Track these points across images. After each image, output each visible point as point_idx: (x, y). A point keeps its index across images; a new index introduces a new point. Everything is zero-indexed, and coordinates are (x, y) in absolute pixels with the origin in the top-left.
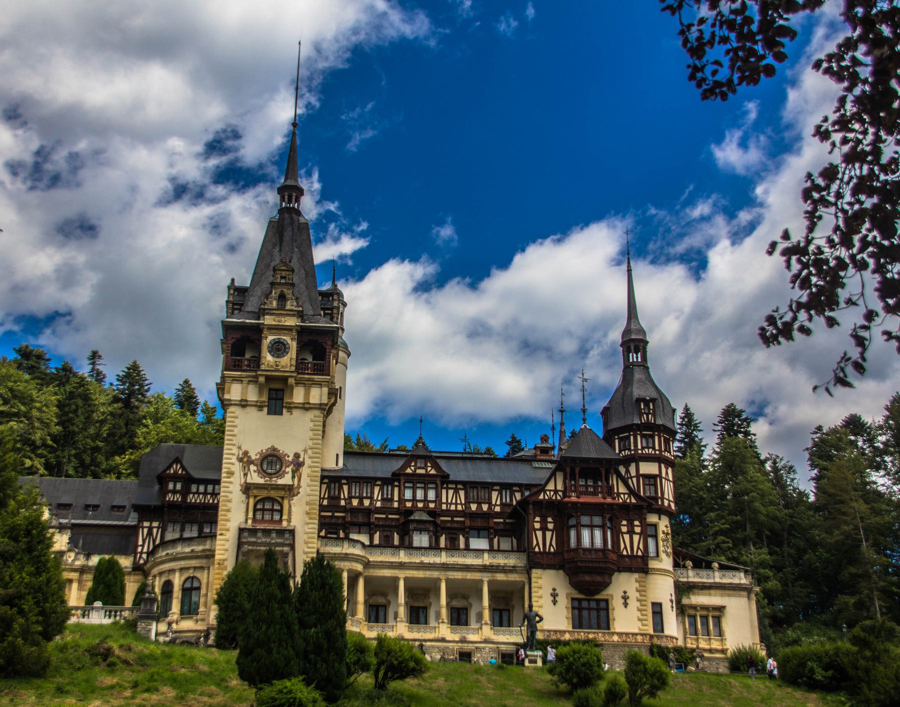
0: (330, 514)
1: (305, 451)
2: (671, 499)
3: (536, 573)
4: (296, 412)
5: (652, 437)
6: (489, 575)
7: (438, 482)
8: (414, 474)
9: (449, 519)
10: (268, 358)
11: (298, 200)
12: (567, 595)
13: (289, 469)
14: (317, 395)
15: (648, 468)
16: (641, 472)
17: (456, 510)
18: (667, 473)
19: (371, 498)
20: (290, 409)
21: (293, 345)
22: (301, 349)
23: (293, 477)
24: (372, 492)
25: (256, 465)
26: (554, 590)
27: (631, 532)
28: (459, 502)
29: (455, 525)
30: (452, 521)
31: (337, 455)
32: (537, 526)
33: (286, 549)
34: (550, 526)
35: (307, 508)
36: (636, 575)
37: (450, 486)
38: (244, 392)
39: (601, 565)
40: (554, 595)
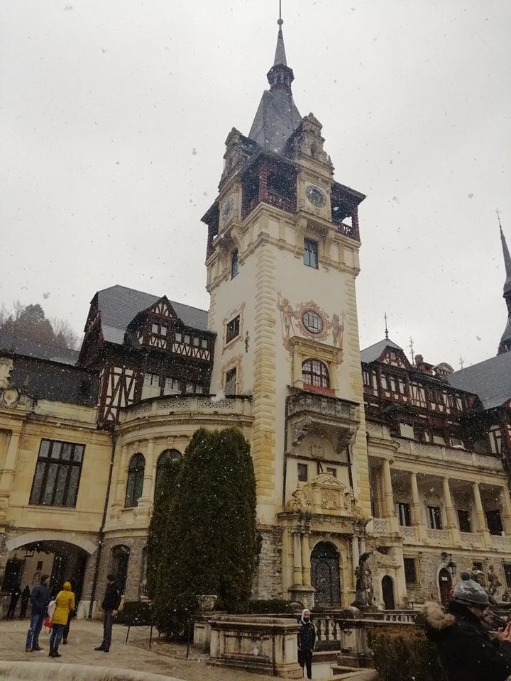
4: (247, 261)
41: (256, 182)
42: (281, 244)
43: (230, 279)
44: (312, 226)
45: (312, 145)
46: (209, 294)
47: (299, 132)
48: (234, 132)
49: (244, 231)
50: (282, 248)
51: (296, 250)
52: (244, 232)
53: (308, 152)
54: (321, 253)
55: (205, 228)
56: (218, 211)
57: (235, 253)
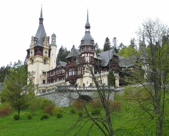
2: (88, 60)
4: (35, 63)
5: (83, 48)
10: (30, 55)
11: (42, 21)
14: (38, 58)
15: (83, 55)
16: (82, 56)
18: (87, 55)
20: (34, 63)
21: (33, 51)
22: (35, 52)
27: (79, 70)
32: (67, 73)
36: (80, 79)
38: (29, 62)
44: (45, 58)
48: (32, 37)
49: (34, 58)
54: (46, 62)
57: (33, 61)
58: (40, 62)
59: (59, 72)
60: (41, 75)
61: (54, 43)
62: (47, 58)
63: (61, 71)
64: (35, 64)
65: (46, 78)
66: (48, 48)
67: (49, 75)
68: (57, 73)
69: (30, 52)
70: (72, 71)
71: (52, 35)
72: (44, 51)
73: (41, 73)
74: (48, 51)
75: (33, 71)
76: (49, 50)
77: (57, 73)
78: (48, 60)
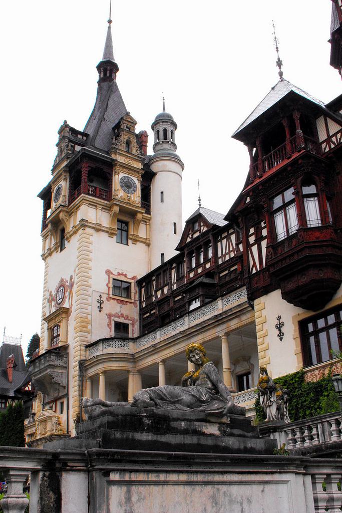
0: (148, 314)
1: (75, 271)
3: (258, 303)
6: (224, 326)
7: (211, 238)
8: (194, 241)
9: (227, 272)
12: (293, 317)
13: (67, 294)
17: (231, 259)
19: (169, 284)
20: (67, 239)
23: (69, 299)
24: (171, 277)
25: (54, 301)
26: (279, 318)
28: (231, 249)
29: (233, 276)
30: (230, 272)
31: (163, 255)
32: (252, 239)
33: (48, 371)
34: (265, 233)
35: (75, 322)
37: (223, 236)
39: (296, 258)
40: (279, 327)
41: (79, 173)
42: (97, 227)
43: (59, 251)
44: (123, 211)
45: (127, 140)
46: (43, 261)
47: (117, 127)
48: (66, 125)
49: (70, 214)
50: (98, 230)
51: (110, 231)
52: (70, 215)
53: (123, 147)
54: (131, 232)
55: (41, 203)
56: (51, 193)
57: (63, 231)
58: (98, 229)
59: (198, 265)
60: (104, 298)
61: (166, 146)
62: (133, 214)
63: (210, 255)
64: (72, 245)
65: (130, 312)
66: (139, 166)
67: (149, 297)
68: (191, 270)
69: (53, 195)
70: (300, 200)
71: (157, 118)
72: (118, 178)
73: (100, 284)
74: (136, 181)
75: (62, 280)
76: (143, 176)
77: (191, 270)
78: (142, 227)
